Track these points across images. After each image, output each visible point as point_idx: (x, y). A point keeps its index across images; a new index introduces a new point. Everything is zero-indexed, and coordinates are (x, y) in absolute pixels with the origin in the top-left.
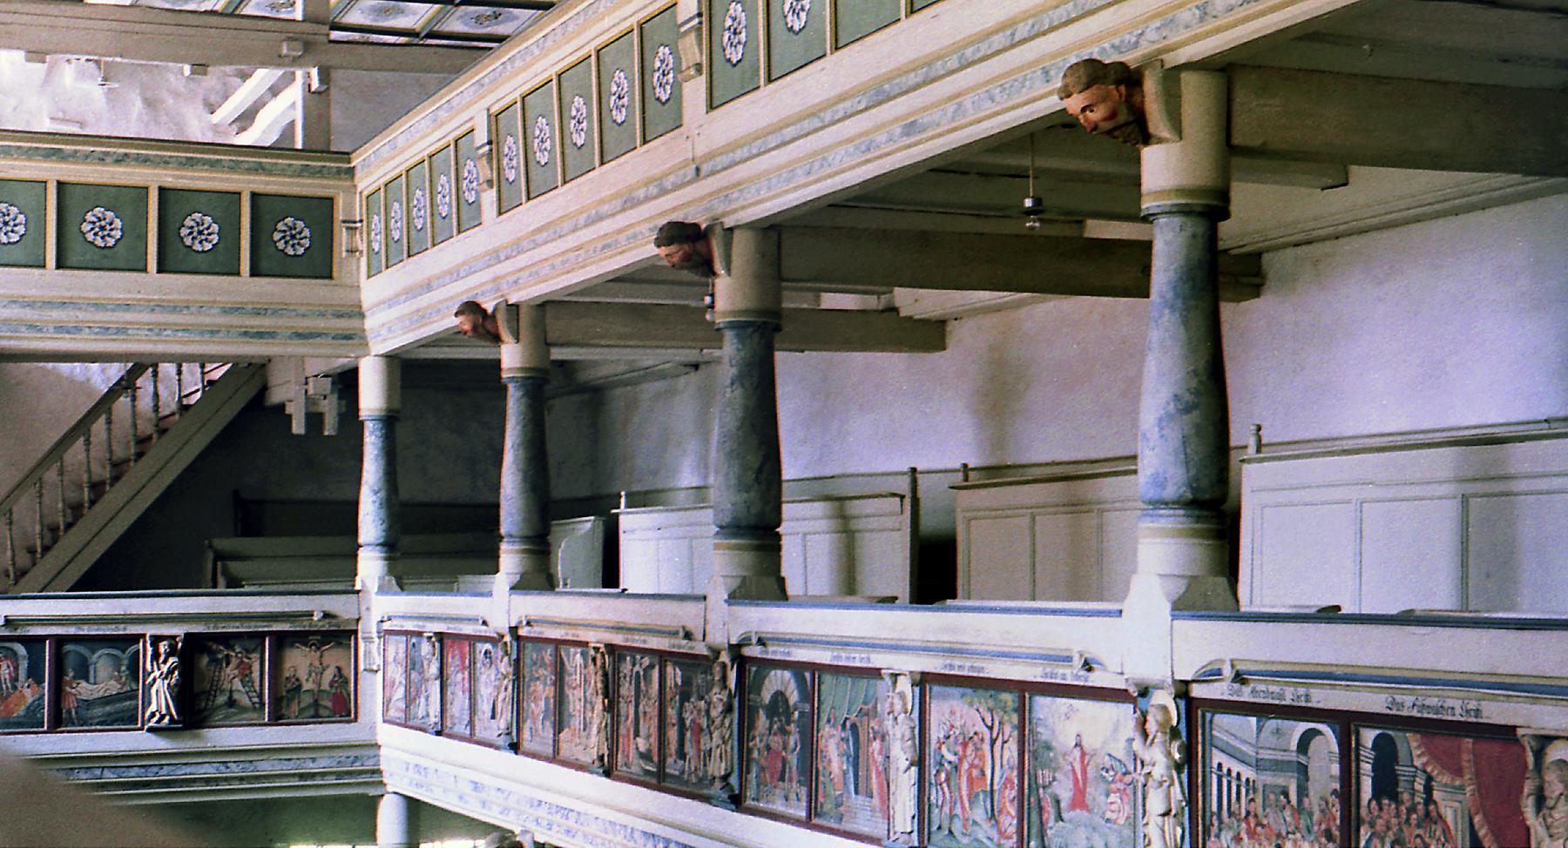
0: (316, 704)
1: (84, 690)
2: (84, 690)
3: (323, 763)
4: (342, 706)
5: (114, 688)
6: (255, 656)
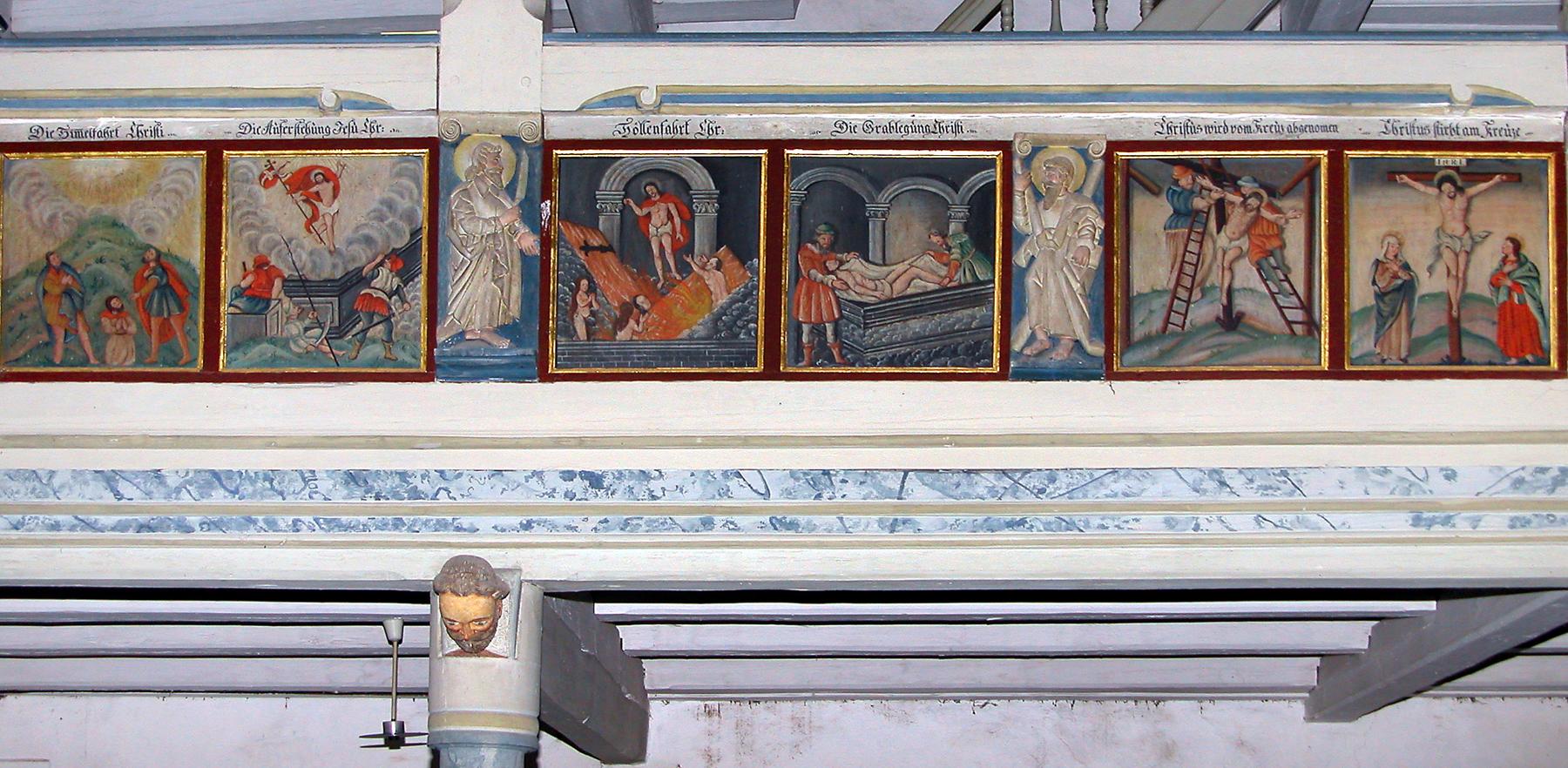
0: (1455, 330)
2: (859, 277)
6: (1293, 205)
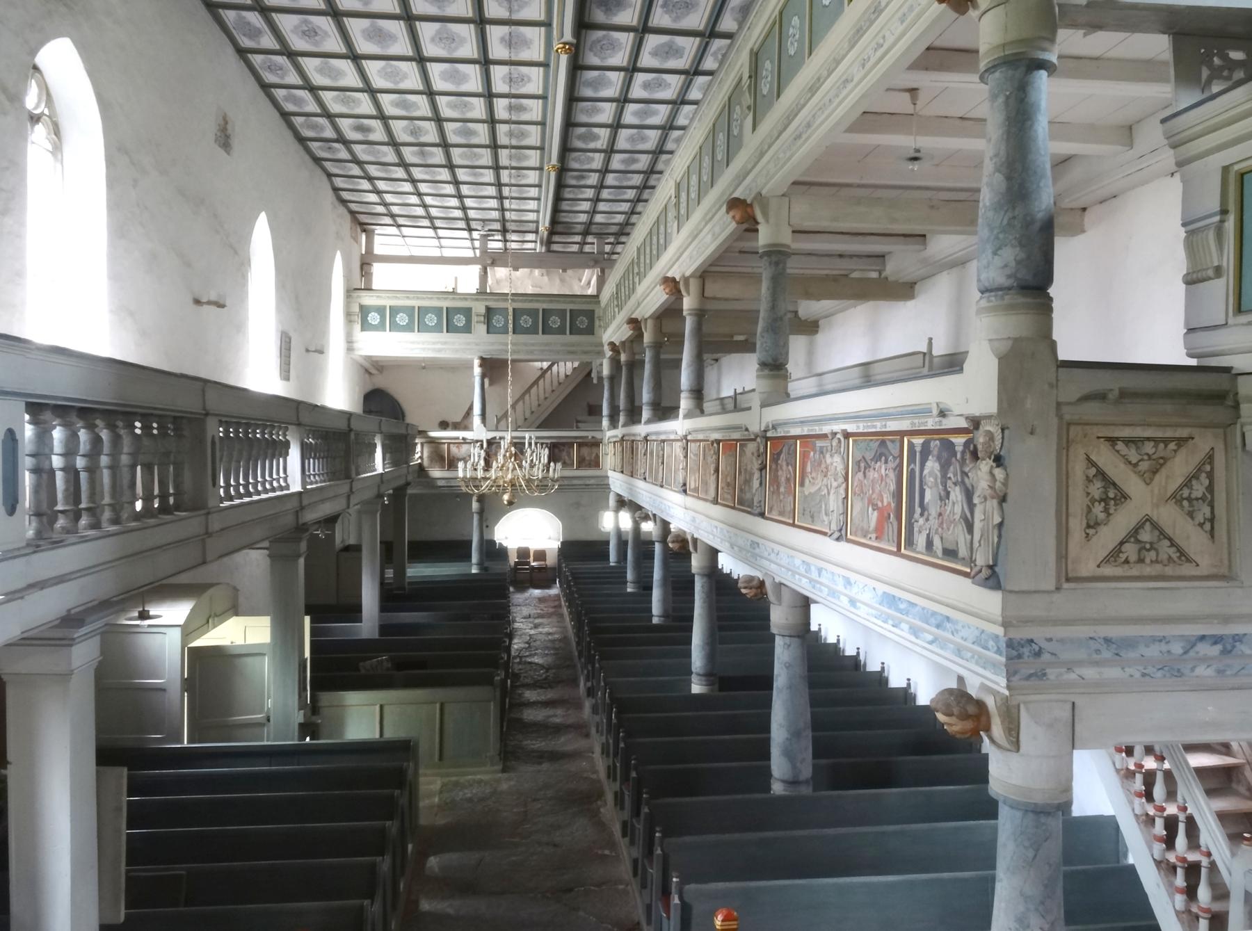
3: (592, 481)
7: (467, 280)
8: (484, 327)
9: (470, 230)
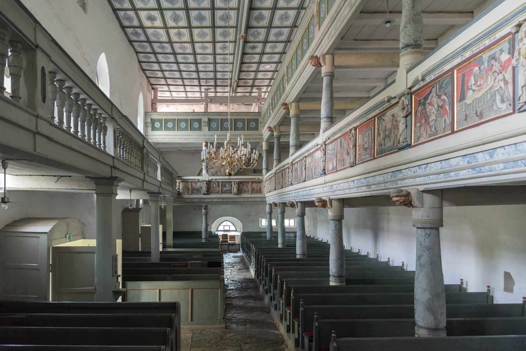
1: (225, 189)
4: (260, 191)
5: (229, 188)
7: (199, 108)
8: (207, 128)
9: (200, 86)
